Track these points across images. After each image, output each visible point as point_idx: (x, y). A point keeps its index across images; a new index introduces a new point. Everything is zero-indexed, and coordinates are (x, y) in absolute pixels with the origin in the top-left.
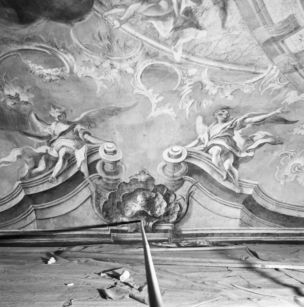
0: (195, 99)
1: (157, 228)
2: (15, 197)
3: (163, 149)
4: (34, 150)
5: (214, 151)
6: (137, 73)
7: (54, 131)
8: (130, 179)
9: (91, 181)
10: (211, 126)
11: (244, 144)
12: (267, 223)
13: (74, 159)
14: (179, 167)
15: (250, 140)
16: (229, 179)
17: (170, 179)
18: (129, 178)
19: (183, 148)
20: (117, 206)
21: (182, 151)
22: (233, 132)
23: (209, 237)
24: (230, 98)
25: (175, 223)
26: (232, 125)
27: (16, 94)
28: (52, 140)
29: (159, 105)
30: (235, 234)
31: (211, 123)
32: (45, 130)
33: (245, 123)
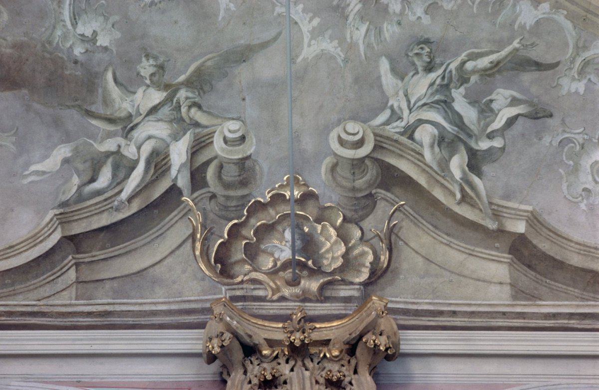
0: (370, 22)
1: (328, 293)
2: (41, 242)
3: (327, 129)
4: (95, 145)
5: (425, 134)
7: (139, 106)
8: (270, 195)
10: (406, 79)
11: (479, 120)
12: (574, 292)
13: (166, 160)
14: (362, 169)
15: (487, 111)
17: (347, 195)
18: (268, 193)
19: (365, 126)
20: (245, 250)
21: (364, 132)
22: (451, 94)
24: (426, 20)
25: (366, 284)
26: (443, 78)
27: (94, 31)
28: (131, 125)
30: (504, 313)
31: (407, 74)
32: (123, 104)
33: (466, 74)
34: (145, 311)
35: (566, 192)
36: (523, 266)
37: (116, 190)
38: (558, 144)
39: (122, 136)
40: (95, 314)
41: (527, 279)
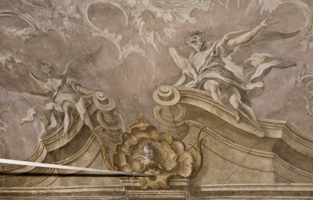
1: (172, 184)
2: (40, 155)
5: (210, 86)
6: (84, 17)
7: (52, 87)
9: (97, 134)
11: (244, 73)
13: (76, 112)
14: (177, 110)
15: (249, 67)
16: (244, 120)
18: (130, 127)
19: (172, 87)
23: (237, 196)
25: (191, 177)
26: (215, 52)
29: (123, 43)
31: (189, 54)
33: (230, 47)
34: (90, 192)
35: (309, 111)
36: (281, 159)
37: (61, 128)
38: (302, 81)
39: (52, 102)
40: (70, 193)
41: (283, 167)
